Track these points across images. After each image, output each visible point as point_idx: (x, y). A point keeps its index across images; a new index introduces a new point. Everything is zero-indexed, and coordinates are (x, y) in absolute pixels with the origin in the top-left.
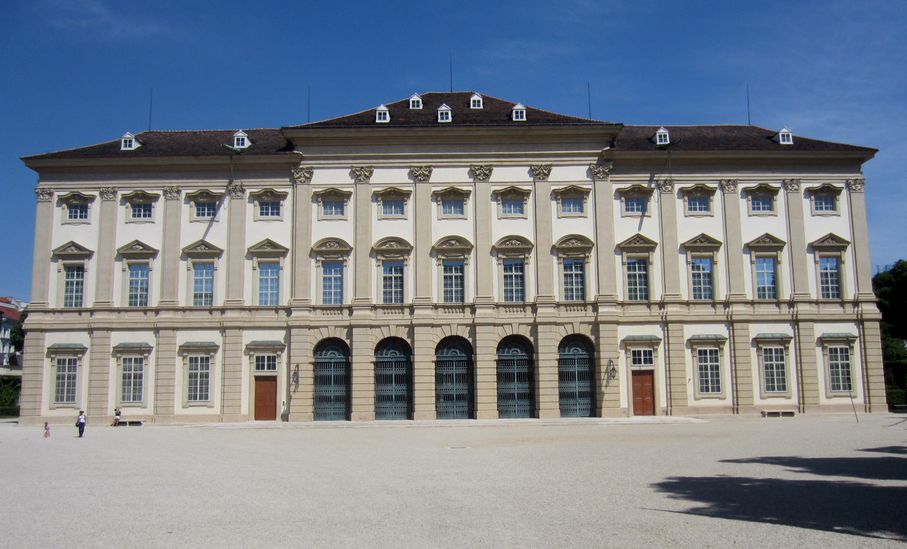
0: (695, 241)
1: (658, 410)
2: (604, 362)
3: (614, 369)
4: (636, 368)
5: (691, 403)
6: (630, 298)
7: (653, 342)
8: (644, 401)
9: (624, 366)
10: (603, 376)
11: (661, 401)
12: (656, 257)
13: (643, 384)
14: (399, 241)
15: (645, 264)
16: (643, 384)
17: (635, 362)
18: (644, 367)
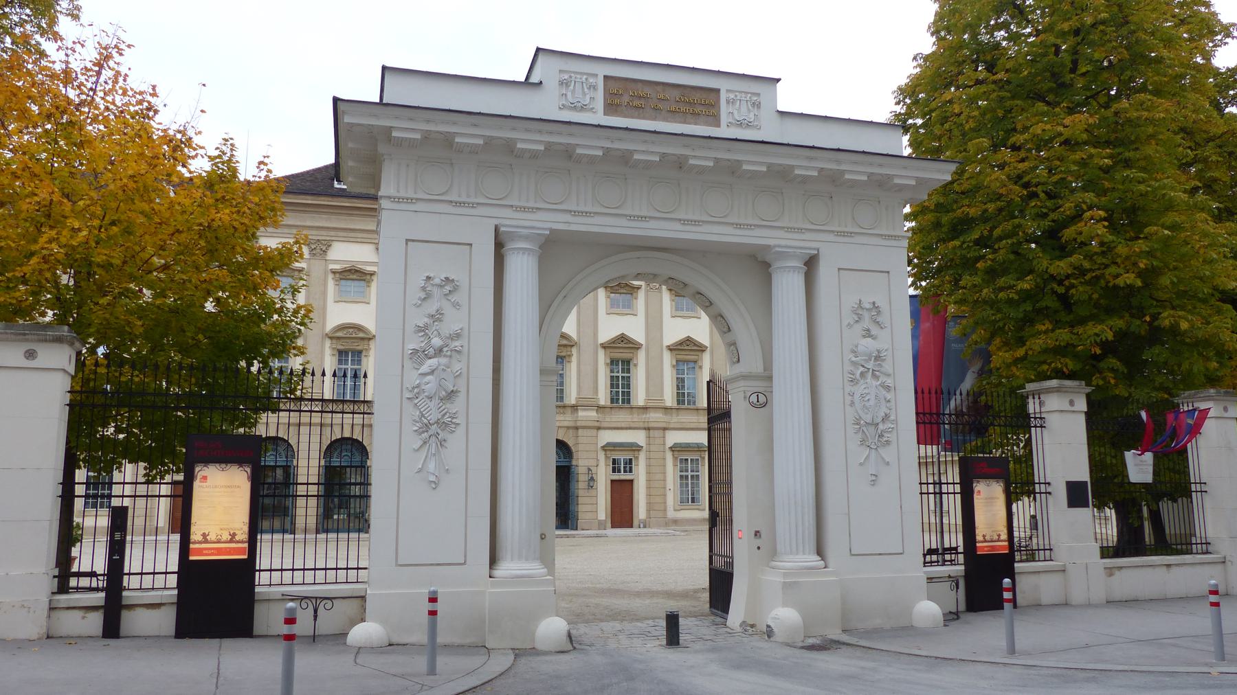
0: (681, 343)
1: (636, 523)
2: (581, 470)
3: (592, 479)
4: (616, 477)
5: (671, 514)
6: (612, 401)
7: (634, 448)
8: (622, 515)
9: (604, 477)
10: (582, 485)
11: (641, 511)
12: (641, 357)
13: (622, 493)
14: (358, 328)
15: (627, 364)
16: (622, 493)
17: (614, 471)
18: (623, 476)
